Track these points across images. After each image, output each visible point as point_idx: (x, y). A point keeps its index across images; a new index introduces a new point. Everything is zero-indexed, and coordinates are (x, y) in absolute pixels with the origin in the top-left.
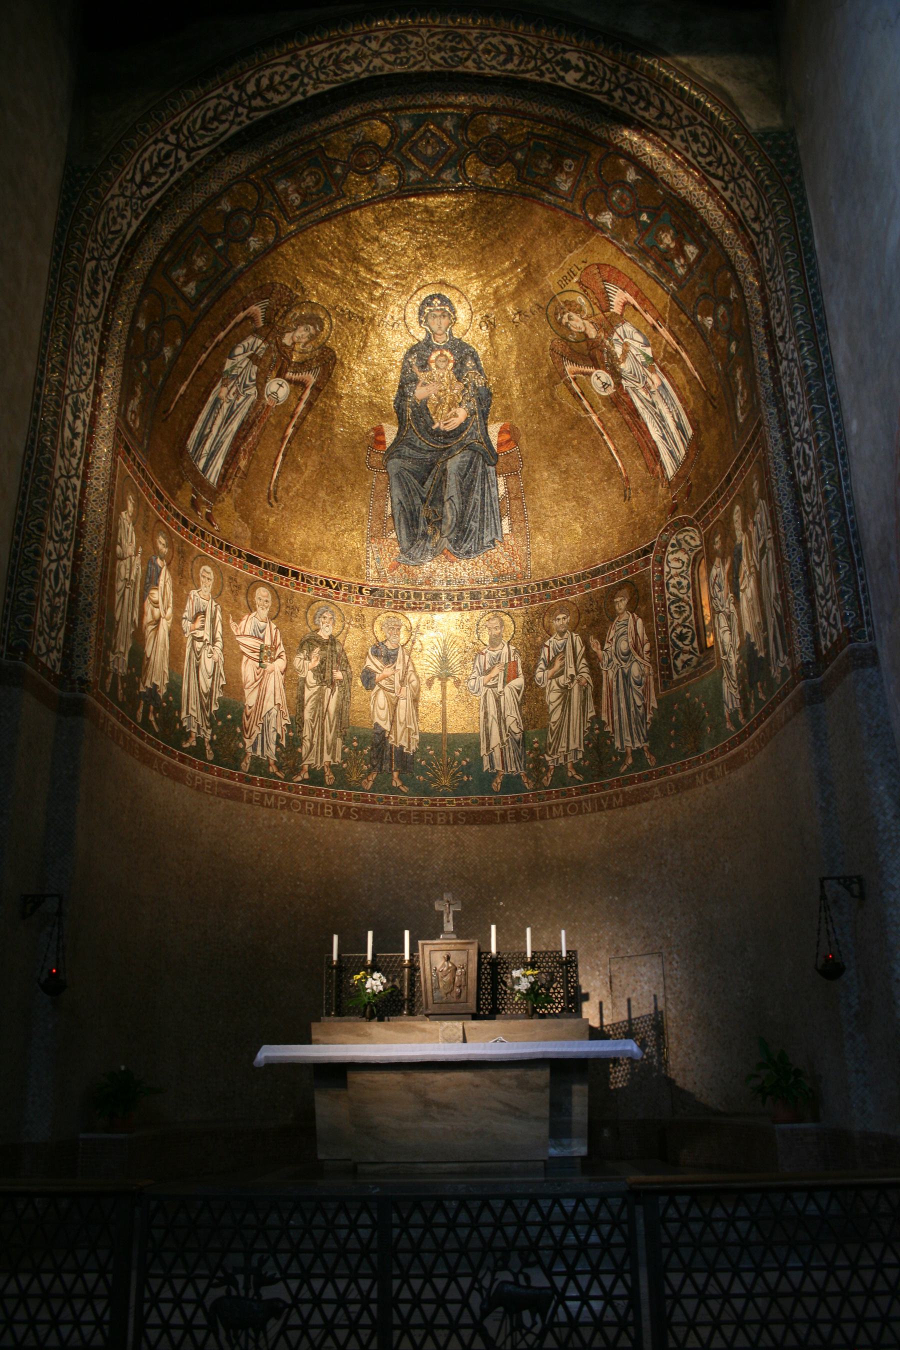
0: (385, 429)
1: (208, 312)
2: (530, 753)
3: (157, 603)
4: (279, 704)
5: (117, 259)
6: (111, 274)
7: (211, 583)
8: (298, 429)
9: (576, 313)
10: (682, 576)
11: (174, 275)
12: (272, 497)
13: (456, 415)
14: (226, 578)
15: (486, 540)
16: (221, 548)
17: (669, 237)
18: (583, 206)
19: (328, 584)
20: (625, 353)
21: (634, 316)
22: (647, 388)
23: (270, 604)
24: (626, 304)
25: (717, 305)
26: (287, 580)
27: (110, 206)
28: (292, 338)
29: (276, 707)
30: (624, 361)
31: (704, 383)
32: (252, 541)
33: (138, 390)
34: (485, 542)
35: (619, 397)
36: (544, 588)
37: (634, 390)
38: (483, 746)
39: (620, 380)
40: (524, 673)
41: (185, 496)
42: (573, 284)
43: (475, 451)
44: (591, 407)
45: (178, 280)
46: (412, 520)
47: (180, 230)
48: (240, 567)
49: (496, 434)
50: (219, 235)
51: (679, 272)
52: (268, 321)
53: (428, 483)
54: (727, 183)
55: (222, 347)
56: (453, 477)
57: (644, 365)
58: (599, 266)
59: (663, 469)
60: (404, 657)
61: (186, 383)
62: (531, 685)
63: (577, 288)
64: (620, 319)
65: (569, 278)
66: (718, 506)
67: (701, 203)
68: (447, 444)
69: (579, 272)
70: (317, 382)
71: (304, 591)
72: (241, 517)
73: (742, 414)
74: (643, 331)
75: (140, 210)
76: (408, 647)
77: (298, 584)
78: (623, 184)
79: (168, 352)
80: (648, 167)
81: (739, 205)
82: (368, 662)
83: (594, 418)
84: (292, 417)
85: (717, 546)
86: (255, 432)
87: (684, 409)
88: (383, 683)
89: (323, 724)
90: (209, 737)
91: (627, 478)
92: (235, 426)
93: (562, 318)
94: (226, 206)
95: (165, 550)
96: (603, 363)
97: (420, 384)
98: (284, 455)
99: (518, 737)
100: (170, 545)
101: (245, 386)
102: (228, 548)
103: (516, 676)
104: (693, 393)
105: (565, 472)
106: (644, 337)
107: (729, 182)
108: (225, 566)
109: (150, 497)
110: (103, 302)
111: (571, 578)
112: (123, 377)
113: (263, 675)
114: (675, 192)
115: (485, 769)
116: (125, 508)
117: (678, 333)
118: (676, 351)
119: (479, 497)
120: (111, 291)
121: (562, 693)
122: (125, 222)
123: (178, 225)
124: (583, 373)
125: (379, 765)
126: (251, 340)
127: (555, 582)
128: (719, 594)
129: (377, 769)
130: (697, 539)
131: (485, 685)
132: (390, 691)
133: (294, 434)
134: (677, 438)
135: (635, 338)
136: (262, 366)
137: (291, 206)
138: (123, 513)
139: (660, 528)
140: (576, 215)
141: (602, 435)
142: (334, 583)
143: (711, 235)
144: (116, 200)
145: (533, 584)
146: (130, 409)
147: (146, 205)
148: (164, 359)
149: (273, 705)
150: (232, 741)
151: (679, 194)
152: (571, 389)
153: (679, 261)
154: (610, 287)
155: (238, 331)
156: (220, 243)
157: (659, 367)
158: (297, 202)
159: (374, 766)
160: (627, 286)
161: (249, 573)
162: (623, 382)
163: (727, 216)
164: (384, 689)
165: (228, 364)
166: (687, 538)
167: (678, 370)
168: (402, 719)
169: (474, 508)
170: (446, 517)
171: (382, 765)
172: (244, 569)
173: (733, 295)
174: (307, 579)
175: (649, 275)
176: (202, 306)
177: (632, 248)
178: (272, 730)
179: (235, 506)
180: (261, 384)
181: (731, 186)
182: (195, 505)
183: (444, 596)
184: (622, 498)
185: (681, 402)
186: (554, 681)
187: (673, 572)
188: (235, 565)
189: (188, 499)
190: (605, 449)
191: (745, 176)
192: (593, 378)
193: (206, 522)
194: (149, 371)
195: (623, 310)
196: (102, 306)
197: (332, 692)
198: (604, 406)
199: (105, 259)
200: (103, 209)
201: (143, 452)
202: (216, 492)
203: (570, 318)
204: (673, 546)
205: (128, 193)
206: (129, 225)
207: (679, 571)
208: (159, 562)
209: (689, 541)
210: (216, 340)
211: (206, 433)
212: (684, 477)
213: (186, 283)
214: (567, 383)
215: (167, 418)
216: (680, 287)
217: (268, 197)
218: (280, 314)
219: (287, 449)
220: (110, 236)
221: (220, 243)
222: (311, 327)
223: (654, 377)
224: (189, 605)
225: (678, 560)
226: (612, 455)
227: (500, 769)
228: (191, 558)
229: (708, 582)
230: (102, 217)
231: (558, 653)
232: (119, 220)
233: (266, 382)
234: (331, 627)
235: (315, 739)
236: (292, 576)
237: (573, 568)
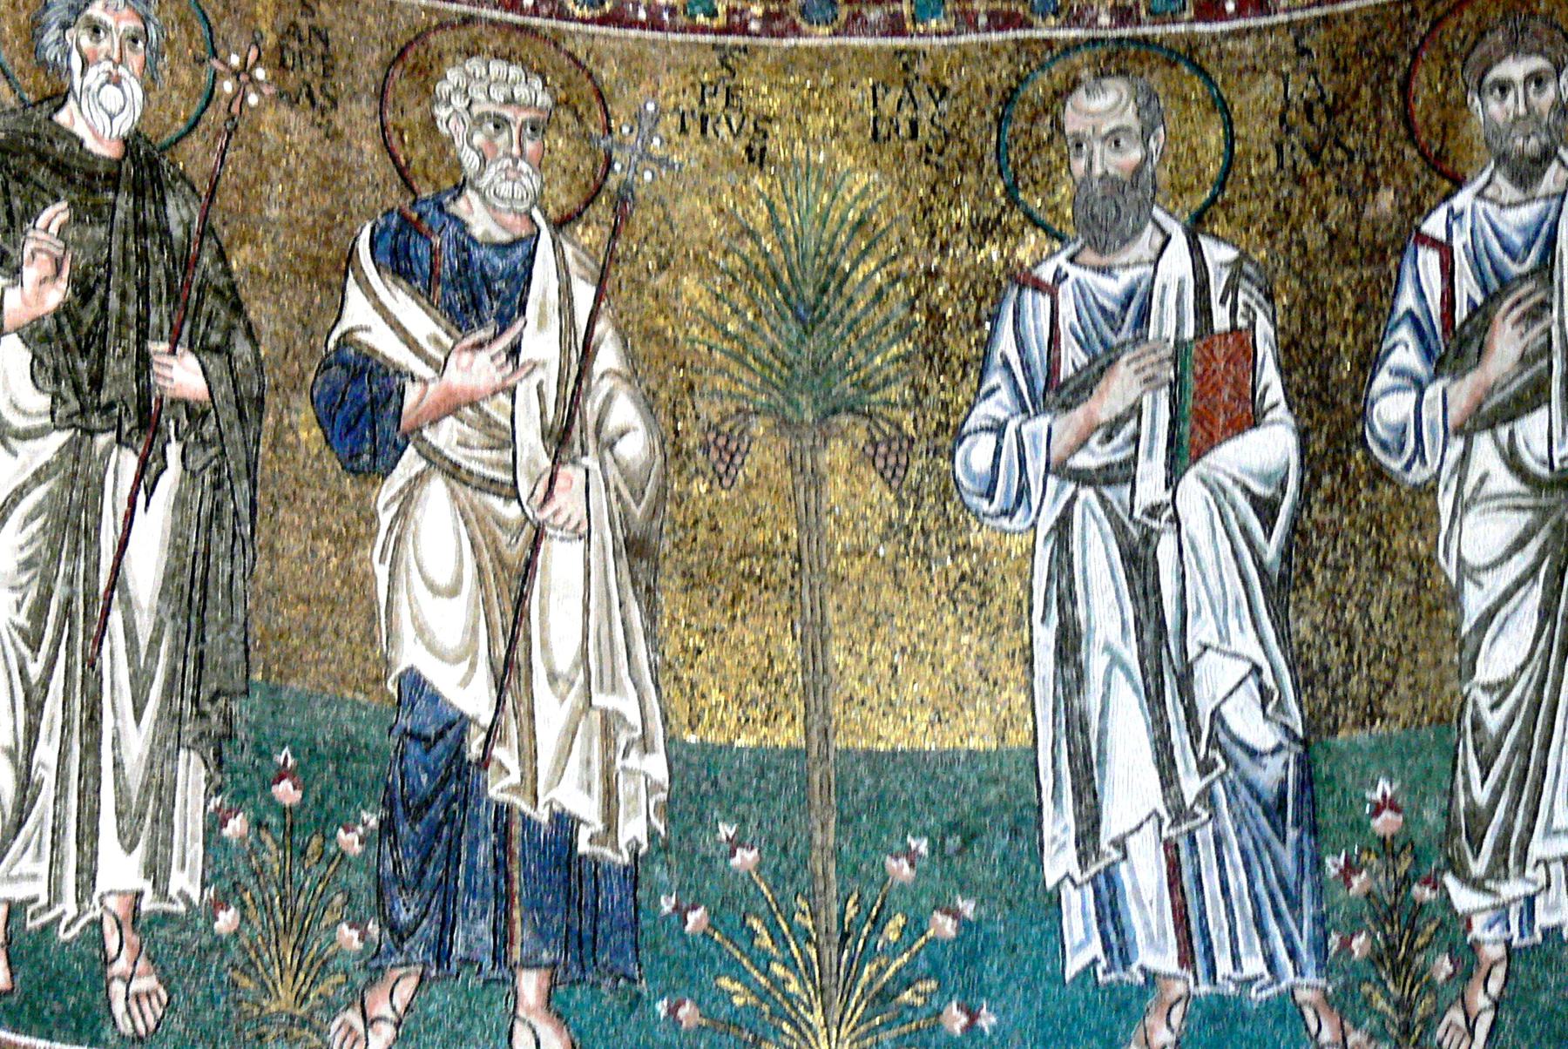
2: (1350, 869)
38: (1059, 825)
40: (1294, 396)
60: (566, 292)
62: (1338, 463)
76: (589, 235)
82: (357, 310)
88: (445, 436)
89: (91, 663)
99: (1269, 774)
103: (1253, 418)
115: (1073, 966)
121: (1543, 513)
125: (429, 928)
129: (417, 948)
131: (1057, 469)
132: (490, 487)
159: (400, 934)
164: (454, 472)
168: (564, 655)
171: (447, 925)
186: (1484, 444)
197: (146, 479)
227: (1166, 961)
231: (1506, 284)
234: (134, 89)
235: (46, 753)
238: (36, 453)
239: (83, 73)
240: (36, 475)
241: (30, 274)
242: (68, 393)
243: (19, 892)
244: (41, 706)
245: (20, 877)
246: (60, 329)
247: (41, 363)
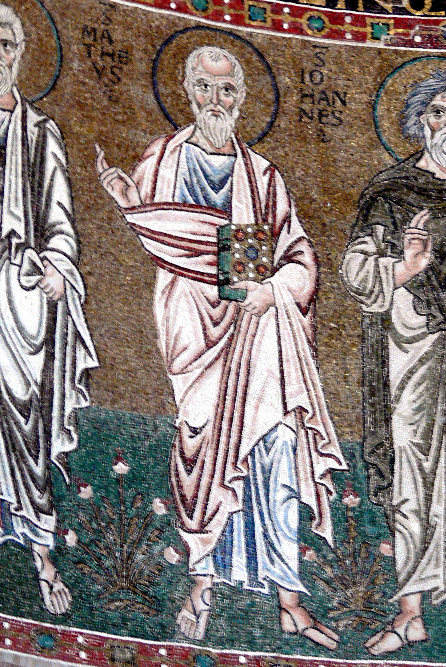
4: (301, 410)
23: (241, 96)
29: (291, 420)
90: (50, 541)
113: (235, 322)
149: (279, 416)
150: (137, 543)
178: (283, 493)
238: (420, 348)
239: (432, 137)
240: (420, 360)
241: (409, 253)
242: (438, 314)
243: (427, 586)
244: (432, 484)
245: (428, 578)
246: (429, 278)
247: (418, 298)
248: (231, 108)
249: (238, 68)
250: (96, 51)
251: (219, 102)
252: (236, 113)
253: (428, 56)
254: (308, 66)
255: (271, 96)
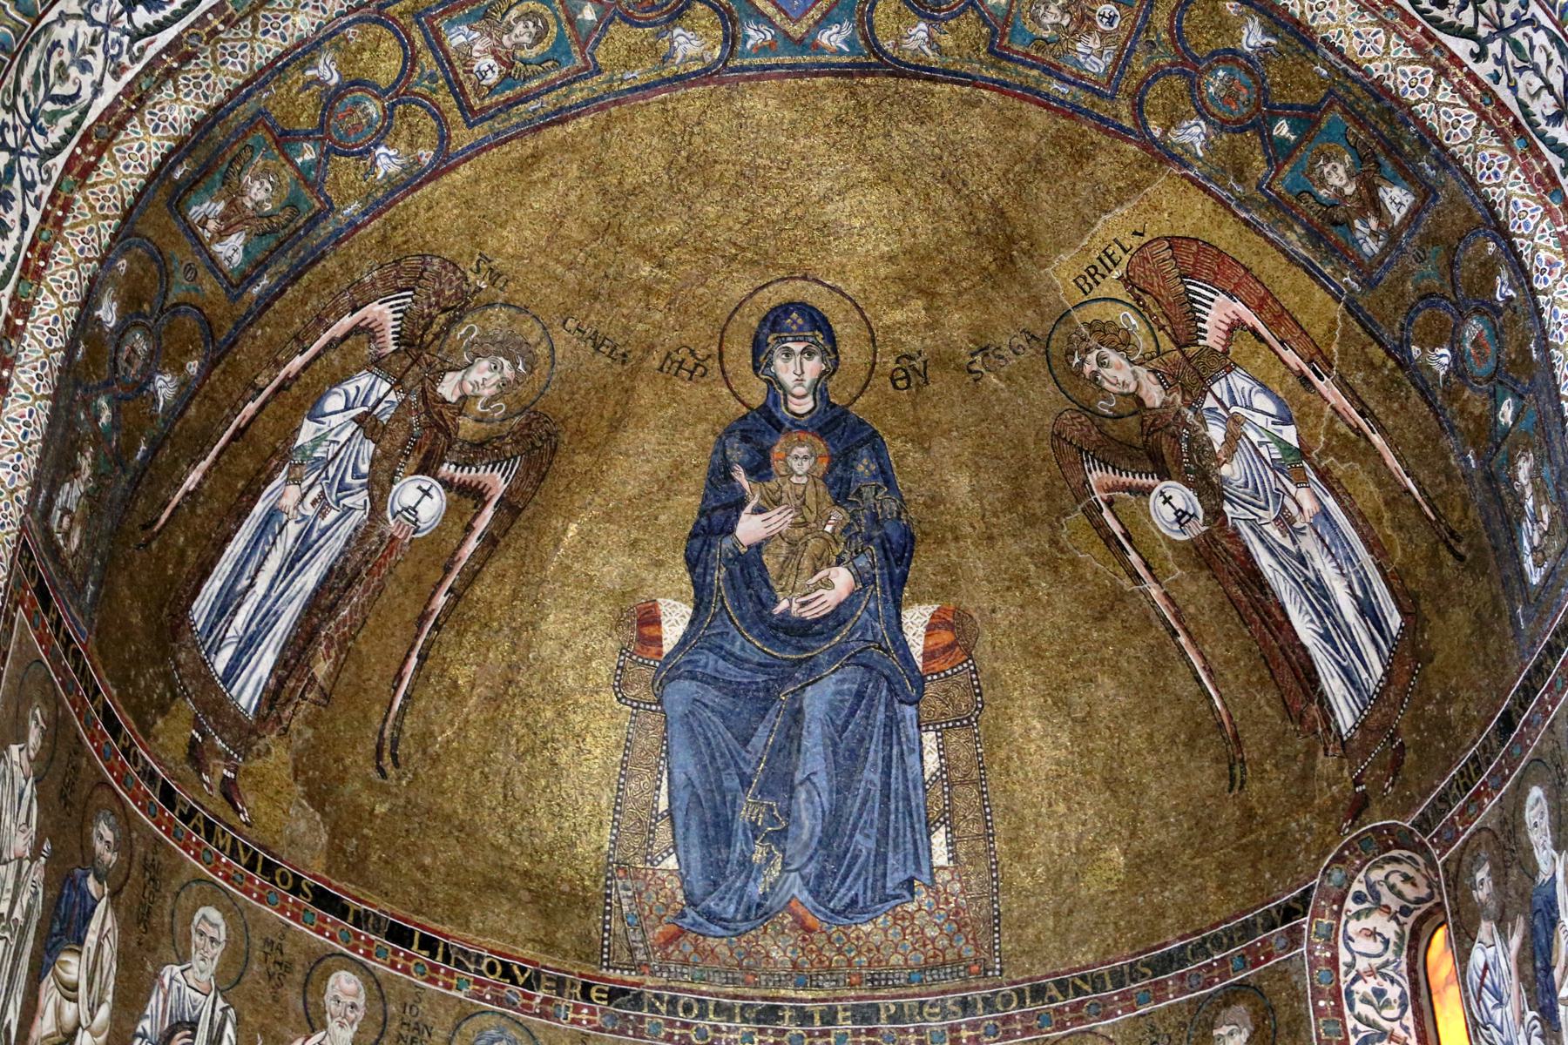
0: (662, 608)
1: (268, 306)
3: (75, 988)
5: (60, 160)
6: (47, 190)
7: (218, 950)
8: (458, 597)
9: (1117, 350)
10: (1384, 976)
11: (195, 212)
12: (386, 754)
13: (827, 584)
14: (258, 943)
15: (894, 879)
16: (251, 866)
17: (1341, 170)
18: (1138, 108)
19: (507, 972)
20: (1232, 440)
21: (1255, 353)
22: (1285, 521)
23: (360, 1014)
24: (1236, 326)
25: (1463, 318)
26: (408, 958)
27: (54, 37)
28: (461, 383)
30: (1230, 457)
31: (1429, 501)
32: (329, 856)
33: (85, 462)
34: (889, 884)
35: (1216, 542)
36: (1034, 1000)
37: (1255, 527)
39: (1220, 505)
41: (175, 731)
42: (1111, 285)
43: (868, 667)
44: (1148, 567)
45: (203, 223)
46: (716, 825)
47: (217, 114)
48: (294, 917)
49: (922, 630)
50: (307, 136)
51: (1366, 248)
52: (406, 341)
53: (757, 741)
54: (1483, 41)
55: (295, 390)
56: (816, 729)
57: (1277, 467)
58: (1173, 242)
59: (1327, 711)
61: (204, 465)
63: (1120, 292)
64: (1224, 362)
65: (1101, 269)
66: (1478, 793)
67: (1422, 91)
68: (806, 650)
69: (1127, 258)
70: (509, 491)
71: (448, 986)
72: (309, 797)
73: (1537, 564)
74: (1276, 387)
75: (125, 59)
77: (435, 969)
78: (1231, 56)
79: (165, 387)
80: (1292, 16)
81: (1514, 89)
83: (1155, 592)
84: (448, 570)
85: (1481, 894)
86: (357, 596)
87: (1379, 567)
91: (1236, 736)
92: (310, 578)
93: (1083, 361)
94: (327, 70)
95: (110, 857)
96: (1179, 463)
97: (748, 509)
98: (422, 658)
100: (123, 845)
101: (343, 487)
102: (269, 868)
104: (1400, 527)
105: (1083, 721)
106: (1277, 400)
107: (1491, 38)
108: (259, 911)
109: (89, 724)
110: (17, 249)
111: (1100, 976)
112: (51, 424)
114: (1358, 68)
116: (21, 738)
117: (1362, 391)
118: (1358, 431)
119: (876, 778)
120: (40, 229)
122: (87, 80)
123: (213, 101)
124: (1129, 489)
126: (364, 381)
127: (1062, 986)
128: (1497, 1015)
130: (1419, 879)
133: (449, 609)
134: (1362, 637)
135: (1256, 405)
136: (386, 444)
137: (477, 88)
138: (14, 749)
139: (1325, 855)
140: (1121, 127)
141: (1175, 634)
142: (523, 970)
143: (1446, 160)
144: (71, 24)
145: (1007, 989)
146: (60, 501)
147: (142, 50)
148: (156, 401)
151: (1367, 73)
152: (1101, 527)
153: (1365, 224)
154: (1198, 289)
155: (334, 355)
156: (309, 154)
157: (1316, 470)
158: (492, 78)
160: (1237, 285)
161: (311, 935)
162: (1227, 508)
163: (1483, 116)
165: (307, 432)
166: (1395, 879)
167: (1362, 476)
169: (864, 803)
170: (798, 822)
172: (304, 923)
173: (1503, 289)
174: (458, 959)
175: (1291, 259)
176: (256, 290)
177: (1249, 199)
179: (296, 770)
180: (379, 485)
181: (1494, 48)
182: (196, 755)
183: (787, 1014)
184: (1225, 783)
185: (1371, 552)
187: (1362, 964)
188: (282, 910)
189: (182, 740)
190: (1181, 668)
191: (1532, 21)
192: (1155, 500)
193: (220, 799)
194: (114, 424)
195: (1229, 341)
196: (14, 260)
198: (1180, 566)
199: (31, 156)
200: (36, 40)
201: (81, 612)
202: (252, 731)
203: (1101, 362)
204: (1359, 898)
205: (101, 16)
206: (98, 89)
207: (1377, 962)
208: (92, 884)
209: (1400, 886)
210: (282, 374)
211: (239, 588)
212: (1383, 728)
213: (221, 235)
214: (1093, 512)
215: (148, 542)
216: (1369, 283)
217: (427, 59)
218: (435, 328)
219: (429, 644)
220: (49, 106)
221: (309, 154)
222: (506, 363)
223: (1303, 495)
224: (155, 1003)
225: (1373, 934)
226: (1199, 680)
228: (175, 884)
229: (1464, 984)
230: (33, 59)
232: (74, 72)
233: (392, 482)
236: (421, 947)
237: (1106, 952)
248: (352, 1023)
249: (362, 992)
250: (271, 959)
251: (345, 1016)
252: (355, 1027)
253: (493, 1012)
254: (410, 1001)
255: (381, 1019)
